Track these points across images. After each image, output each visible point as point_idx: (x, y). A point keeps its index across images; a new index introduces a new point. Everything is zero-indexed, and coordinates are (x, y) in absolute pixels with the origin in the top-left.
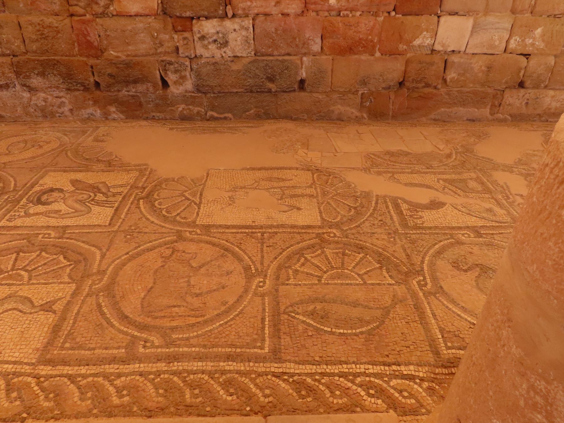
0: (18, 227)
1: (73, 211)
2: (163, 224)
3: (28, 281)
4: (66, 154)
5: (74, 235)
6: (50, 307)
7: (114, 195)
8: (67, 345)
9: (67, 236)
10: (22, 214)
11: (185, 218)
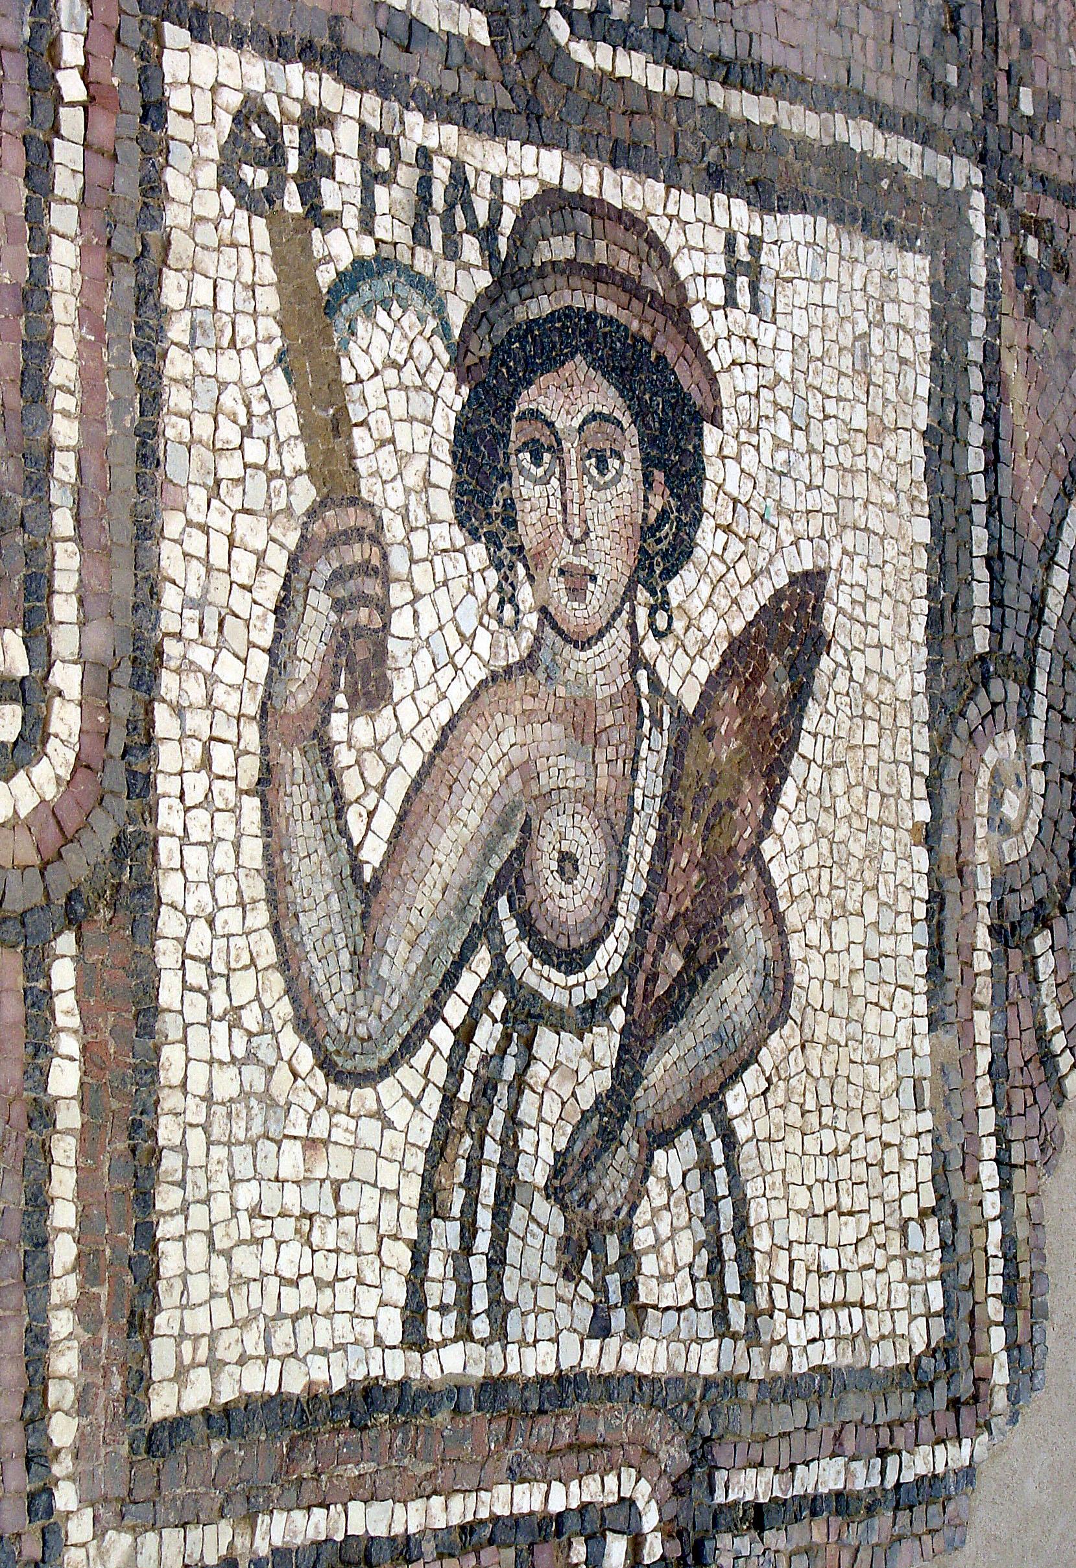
1: (373, 853)
10: (340, 248)
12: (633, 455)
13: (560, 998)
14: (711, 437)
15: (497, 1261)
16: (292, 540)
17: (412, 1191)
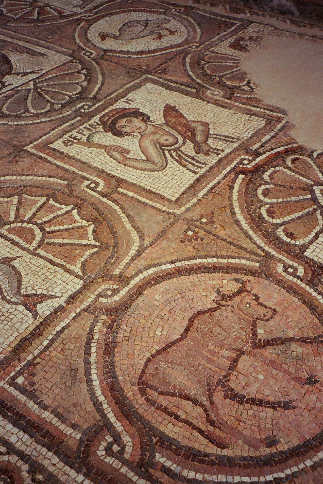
0: (69, 157)
1: (144, 158)
2: (251, 233)
3: (36, 249)
4: (184, 59)
5: (124, 198)
6: (35, 305)
7: (207, 154)
8: (20, 380)
9: (115, 196)
10: (84, 139)
11: (291, 236)
12: (134, 119)
13: (179, 146)
14: (141, 111)
15: (198, 162)
16: (106, 153)
17: (181, 167)
